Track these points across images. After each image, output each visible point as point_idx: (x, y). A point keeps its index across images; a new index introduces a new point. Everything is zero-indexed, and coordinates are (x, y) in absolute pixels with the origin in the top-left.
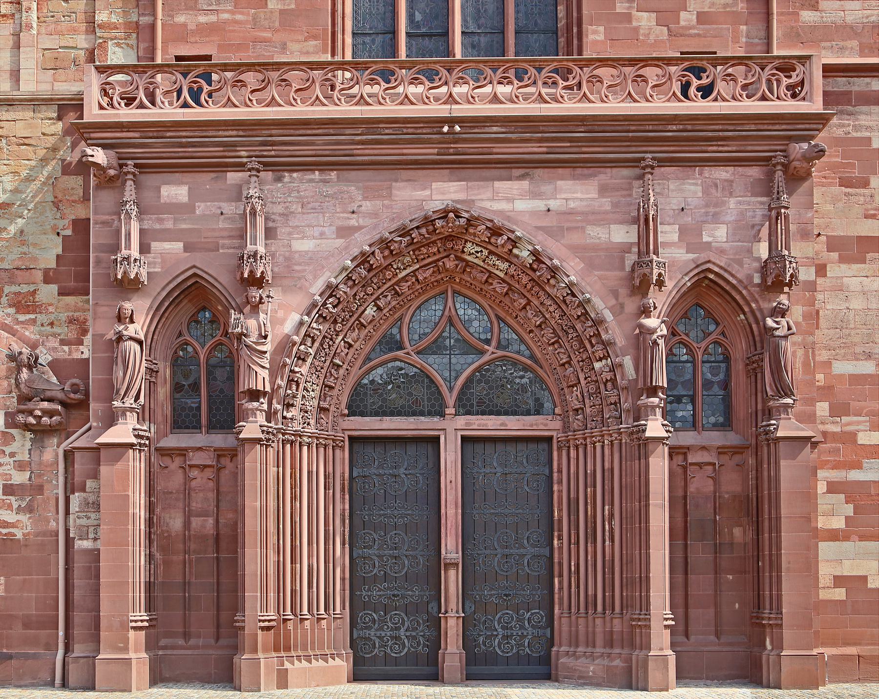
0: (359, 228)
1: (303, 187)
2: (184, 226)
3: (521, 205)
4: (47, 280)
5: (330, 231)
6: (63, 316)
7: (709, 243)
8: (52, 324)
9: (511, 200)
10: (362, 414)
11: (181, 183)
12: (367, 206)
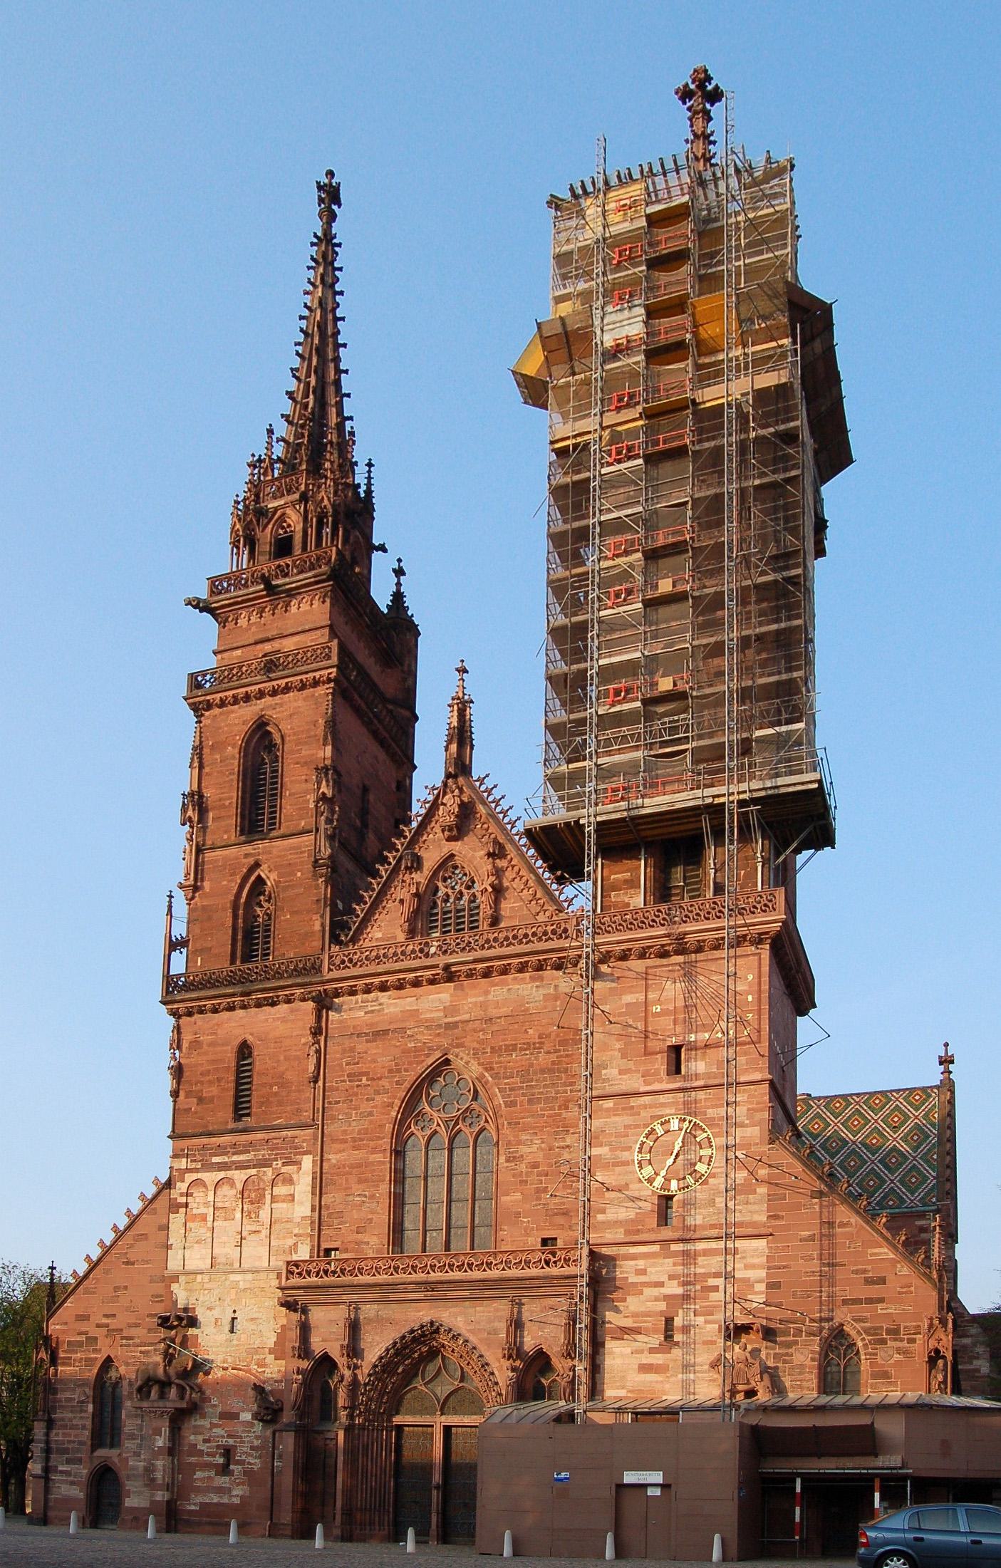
6: (276, 1369)
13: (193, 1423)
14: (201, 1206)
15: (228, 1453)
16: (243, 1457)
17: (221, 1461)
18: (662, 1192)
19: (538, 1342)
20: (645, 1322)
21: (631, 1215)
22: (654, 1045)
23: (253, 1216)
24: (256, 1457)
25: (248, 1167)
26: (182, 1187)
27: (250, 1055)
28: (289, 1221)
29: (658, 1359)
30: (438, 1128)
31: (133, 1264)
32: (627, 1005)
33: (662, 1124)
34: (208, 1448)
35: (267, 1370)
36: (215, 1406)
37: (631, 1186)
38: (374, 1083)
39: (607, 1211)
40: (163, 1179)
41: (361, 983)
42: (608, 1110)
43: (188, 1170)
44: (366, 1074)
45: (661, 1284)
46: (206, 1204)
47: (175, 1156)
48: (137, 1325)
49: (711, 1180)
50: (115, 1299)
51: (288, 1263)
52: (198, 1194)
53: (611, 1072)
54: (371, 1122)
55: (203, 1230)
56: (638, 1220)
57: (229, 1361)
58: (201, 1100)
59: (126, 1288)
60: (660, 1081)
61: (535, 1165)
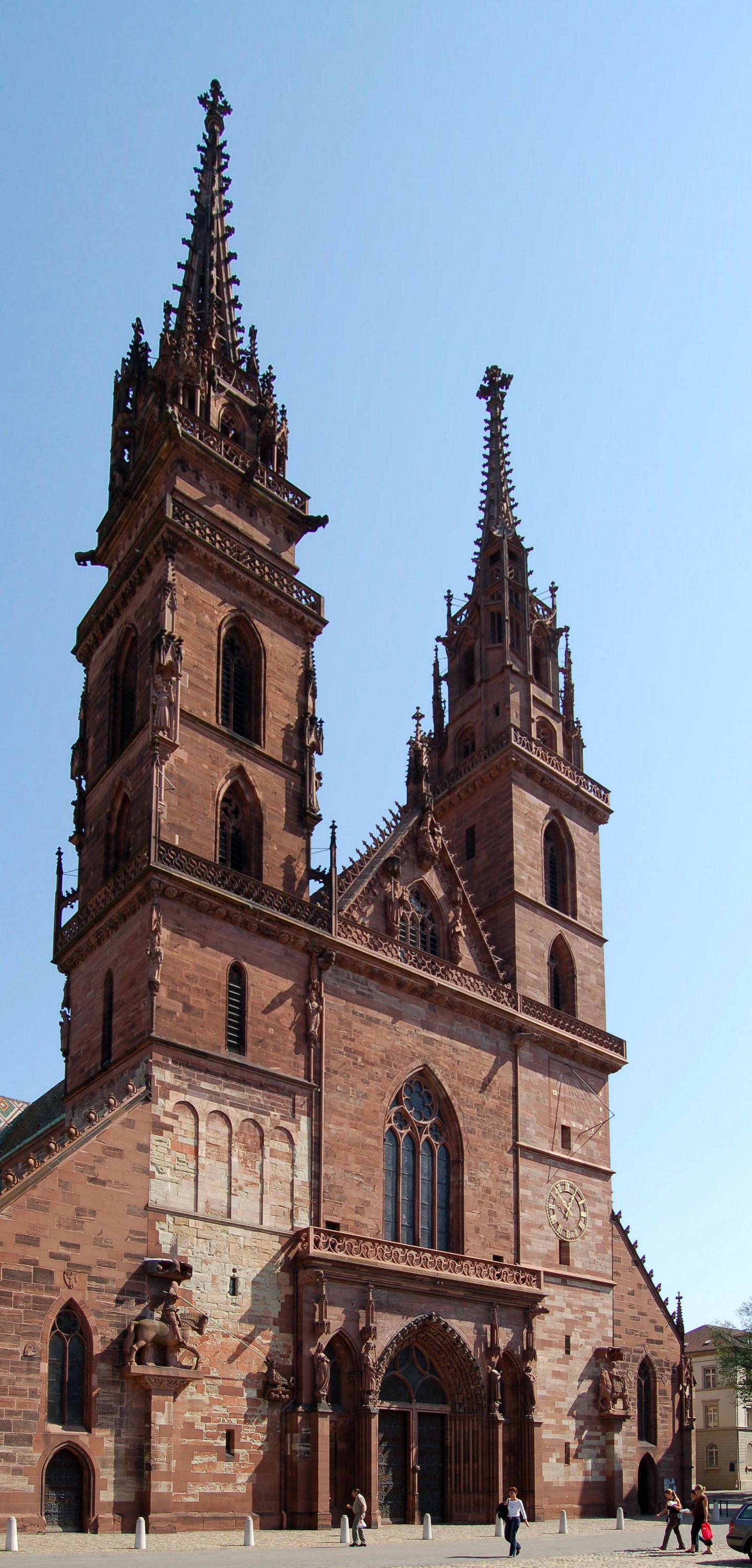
13: (188, 1397)
15: (230, 1435)
23: (250, 1165)
25: (245, 1108)
26: (169, 1105)
31: (104, 1183)
38: (369, 1067)
43: (177, 1089)
44: (362, 1054)
48: (110, 1265)
50: (77, 1225)
54: (367, 1104)
58: (187, 1008)
59: (93, 1213)
61: (488, 1191)
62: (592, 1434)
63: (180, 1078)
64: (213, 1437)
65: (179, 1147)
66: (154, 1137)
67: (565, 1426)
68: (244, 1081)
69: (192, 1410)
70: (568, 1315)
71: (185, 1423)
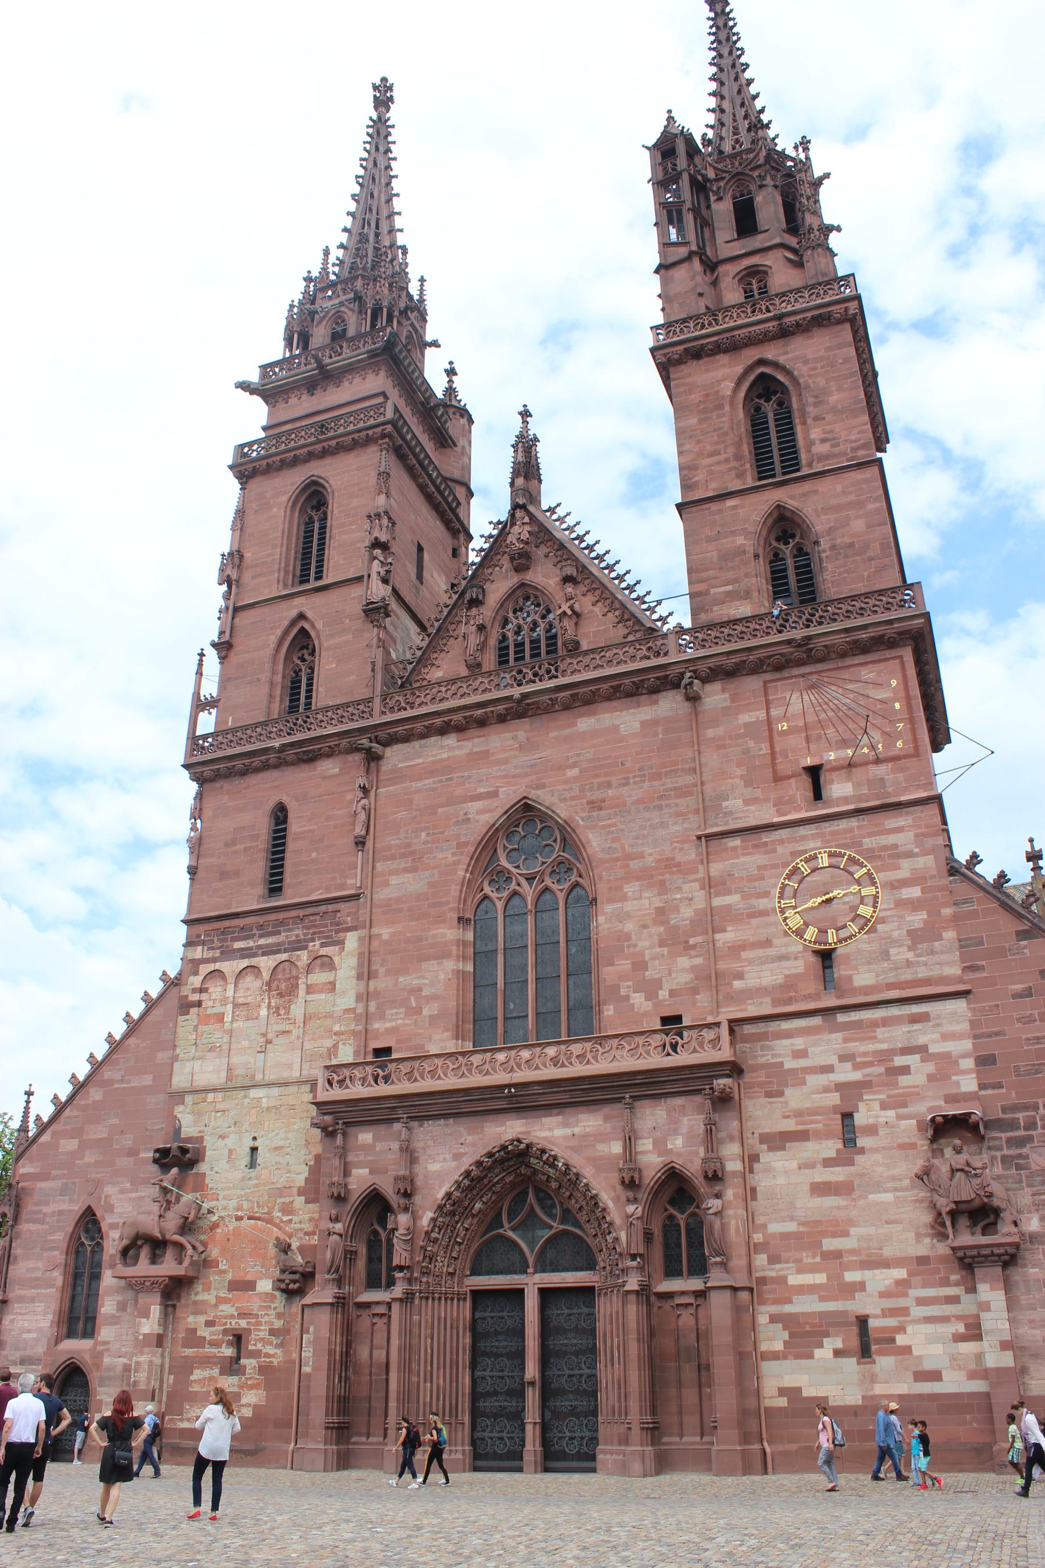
0: (463, 1155)
1: (435, 1129)
2: (370, 1158)
3: (558, 1132)
4: (299, 1194)
5: (448, 1157)
6: (307, 1217)
7: (671, 1149)
8: (300, 1222)
9: (551, 1130)
10: (480, 1274)
11: (369, 1131)
12: (470, 1139)
14: (218, 1004)
16: (259, 1346)
17: (229, 1352)
18: (817, 946)
19: (668, 1159)
20: (813, 1122)
21: (780, 980)
22: (784, 767)
23: (282, 1012)
24: (277, 1346)
27: (285, 820)
28: (329, 1015)
29: (837, 1174)
30: (517, 888)
32: (746, 725)
33: (807, 861)
34: (212, 1333)
35: (295, 1218)
36: (224, 1272)
37: (776, 942)
39: (746, 976)
40: (172, 974)
41: (419, 726)
42: (735, 848)
45: (829, 1069)
46: (224, 1001)
47: (189, 944)
49: (879, 927)
51: (327, 1067)
52: (215, 990)
53: (734, 804)
55: (218, 1035)
56: (790, 984)
57: (245, 1206)
60: (798, 809)
62: (932, 1292)
63: (213, 949)
64: (213, 1344)
65: (205, 1020)
66: (181, 1018)
67: (854, 1283)
68: (282, 923)
69: (196, 1313)
70: (846, 1074)
71: (187, 1329)
